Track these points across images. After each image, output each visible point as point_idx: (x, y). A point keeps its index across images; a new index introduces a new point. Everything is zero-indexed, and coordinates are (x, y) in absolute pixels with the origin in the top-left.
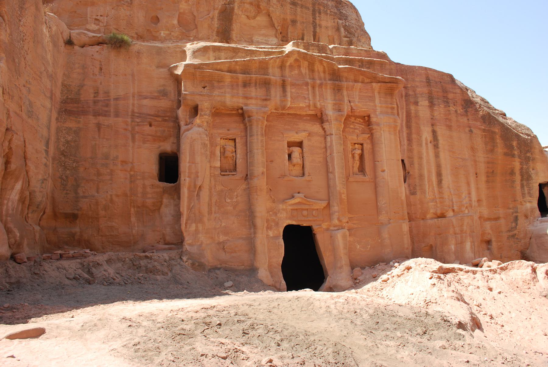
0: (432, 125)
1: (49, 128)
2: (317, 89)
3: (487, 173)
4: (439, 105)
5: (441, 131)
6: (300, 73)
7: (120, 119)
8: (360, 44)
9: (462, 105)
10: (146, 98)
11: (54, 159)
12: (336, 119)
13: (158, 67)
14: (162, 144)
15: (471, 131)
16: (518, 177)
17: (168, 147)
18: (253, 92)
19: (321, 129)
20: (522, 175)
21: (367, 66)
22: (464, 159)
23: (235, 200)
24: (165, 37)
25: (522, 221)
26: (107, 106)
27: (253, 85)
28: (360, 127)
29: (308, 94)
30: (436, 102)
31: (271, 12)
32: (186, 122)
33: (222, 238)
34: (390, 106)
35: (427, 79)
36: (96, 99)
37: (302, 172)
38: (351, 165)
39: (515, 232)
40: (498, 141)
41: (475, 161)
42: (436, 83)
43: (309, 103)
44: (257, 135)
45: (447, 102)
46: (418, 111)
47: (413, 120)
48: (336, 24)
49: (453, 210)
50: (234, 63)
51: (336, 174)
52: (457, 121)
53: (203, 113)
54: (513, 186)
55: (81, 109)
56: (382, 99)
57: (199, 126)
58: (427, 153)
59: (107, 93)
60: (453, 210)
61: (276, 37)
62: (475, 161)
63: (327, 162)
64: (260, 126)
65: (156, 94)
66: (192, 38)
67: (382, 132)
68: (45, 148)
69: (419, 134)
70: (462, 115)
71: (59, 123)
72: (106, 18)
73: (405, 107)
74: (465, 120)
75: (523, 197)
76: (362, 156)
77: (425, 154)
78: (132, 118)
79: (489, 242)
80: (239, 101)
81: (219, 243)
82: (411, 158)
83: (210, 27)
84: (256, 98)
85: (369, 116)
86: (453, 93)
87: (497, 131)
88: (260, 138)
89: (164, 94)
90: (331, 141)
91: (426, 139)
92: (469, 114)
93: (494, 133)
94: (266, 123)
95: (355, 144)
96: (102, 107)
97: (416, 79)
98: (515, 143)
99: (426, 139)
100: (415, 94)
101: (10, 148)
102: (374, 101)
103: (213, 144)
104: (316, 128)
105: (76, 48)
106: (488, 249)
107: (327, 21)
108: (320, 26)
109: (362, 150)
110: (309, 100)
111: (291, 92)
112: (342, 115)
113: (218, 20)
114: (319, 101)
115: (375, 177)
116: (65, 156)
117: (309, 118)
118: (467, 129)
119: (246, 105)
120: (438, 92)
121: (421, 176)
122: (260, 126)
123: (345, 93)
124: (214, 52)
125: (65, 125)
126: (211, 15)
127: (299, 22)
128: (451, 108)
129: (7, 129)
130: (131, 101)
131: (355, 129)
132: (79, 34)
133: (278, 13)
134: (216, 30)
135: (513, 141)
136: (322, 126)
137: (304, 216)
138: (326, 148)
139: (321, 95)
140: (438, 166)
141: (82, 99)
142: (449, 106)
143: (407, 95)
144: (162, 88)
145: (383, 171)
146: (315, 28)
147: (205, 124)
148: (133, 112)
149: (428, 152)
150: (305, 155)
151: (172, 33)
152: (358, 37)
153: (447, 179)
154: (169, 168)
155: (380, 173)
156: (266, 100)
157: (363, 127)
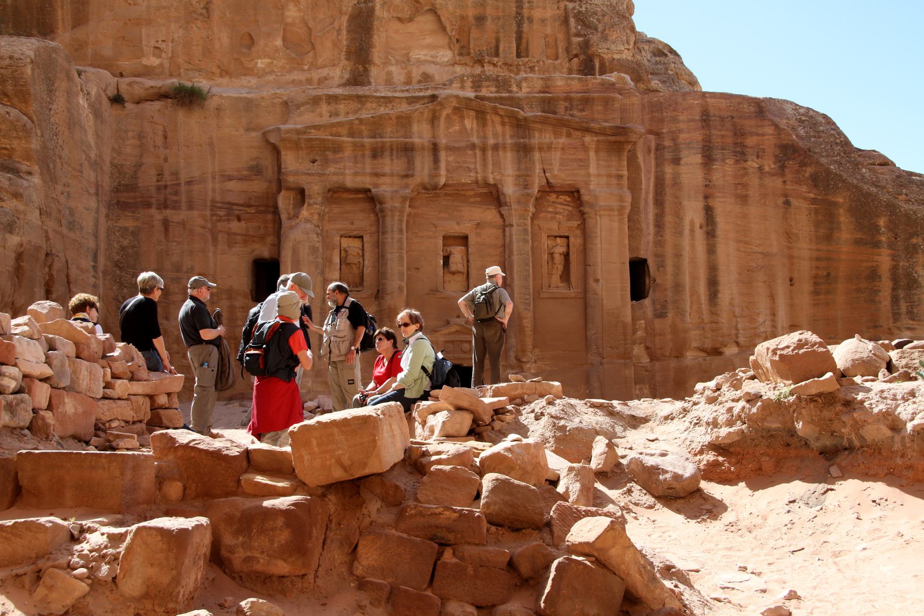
0: (706, 197)
1: (96, 236)
2: (489, 154)
3: (816, 277)
4: (723, 160)
5: (724, 207)
6: (463, 129)
7: (195, 213)
8: (604, 45)
9: (776, 156)
10: (230, 180)
11: (105, 273)
12: (519, 202)
13: (248, 130)
14: (256, 246)
15: (787, 203)
16: (885, 285)
17: (265, 252)
19: (498, 216)
20: (895, 279)
21: (580, 107)
22: (766, 255)
24: (263, 69)
26: (176, 193)
27: (387, 153)
28: (565, 210)
29: (475, 163)
30: (717, 154)
31: (438, 7)
32: (289, 214)
34: (614, 172)
35: (703, 115)
36: (160, 183)
37: (465, 284)
38: (545, 270)
40: (842, 219)
41: (791, 257)
42: (722, 119)
43: (477, 177)
44: (392, 231)
45: (741, 154)
46: (679, 174)
47: (669, 191)
48: (562, 11)
49: (737, 344)
50: (357, 122)
52: (762, 186)
53: (312, 201)
54: (873, 301)
55: (139, 200)
56: (602, 163)
57: (307, 221)
58: (693, 247)
59: (175, 174)
60: (737, 344)
61: (450, 49)
62: (791, 257)
64: (396, 218)
65: (246, 173)
66: (306, 67)
67: (598, 218)
68: (92, 264)
69: (678, 215)
70: (773, 175)
71: (110, 222)
72: (171, 44)
73: (653, 170)
74: (778, 182)
75: (896, 320)
76: (567, 256)
78: (212, 210)
80: (366, 181)
82: (660, 256)
83: (335, 45)
84: (392, 175)
85: (578, 191)
86: (758, 135)
87: (841, 200)
88: (396, 236)
89: (256, 171)
90: (511, 236)
91: (692, 223)
92: (787, 171)
93: (836, 204)
94: (408, 210)
95: (556, 237)
96: (168, 195)
97: (681, 118)
98: (882, 222)
99: (692, 223)
100: (676, 145)
101: (51, 276)
102: (587, 167)
103: (328, 246)
104: (490, 215)
105: (129, 106)
107: (545, 8)
108: (530, 20)
109: (568, 246)
110: (477, 173)
111: (447, 161)
112: (528, 195)
113: (348, 32)
114: (492, 173)
115: (585, 290)
116: (120, 268)
117: (479, 199)
118: (780, 201)
119: (377, 186)
120: (723, 136)
121: (678, 287)
122: (396, 218)
123: (537, 156)
124: (329, 104)
125: (118, 224)
126: (336, 25)
127: (489, 19)
128: (749, 163)
129: (47, 255)
130: (210, 185)
131: (556, 213)
132: (130, 84)
133: (450, 8)
134: (345, 49)
135: (878, 216)
136: (500, 212)
137: (464, 352)
139: (497, 164)
141: (140, 185)
142: (745, 161)
143: (659, 148)
144: (254, 163)
145: (597, 281)
146: (519, 24)
147: (316, 217)
148: (213, 201)
149: (693, 246)
150: (471, 258)
151: (275, 62)
152: (602, 33)
153: (729, 290)
155: (592, 283)
156: (406, 176)
157: (570, 209)
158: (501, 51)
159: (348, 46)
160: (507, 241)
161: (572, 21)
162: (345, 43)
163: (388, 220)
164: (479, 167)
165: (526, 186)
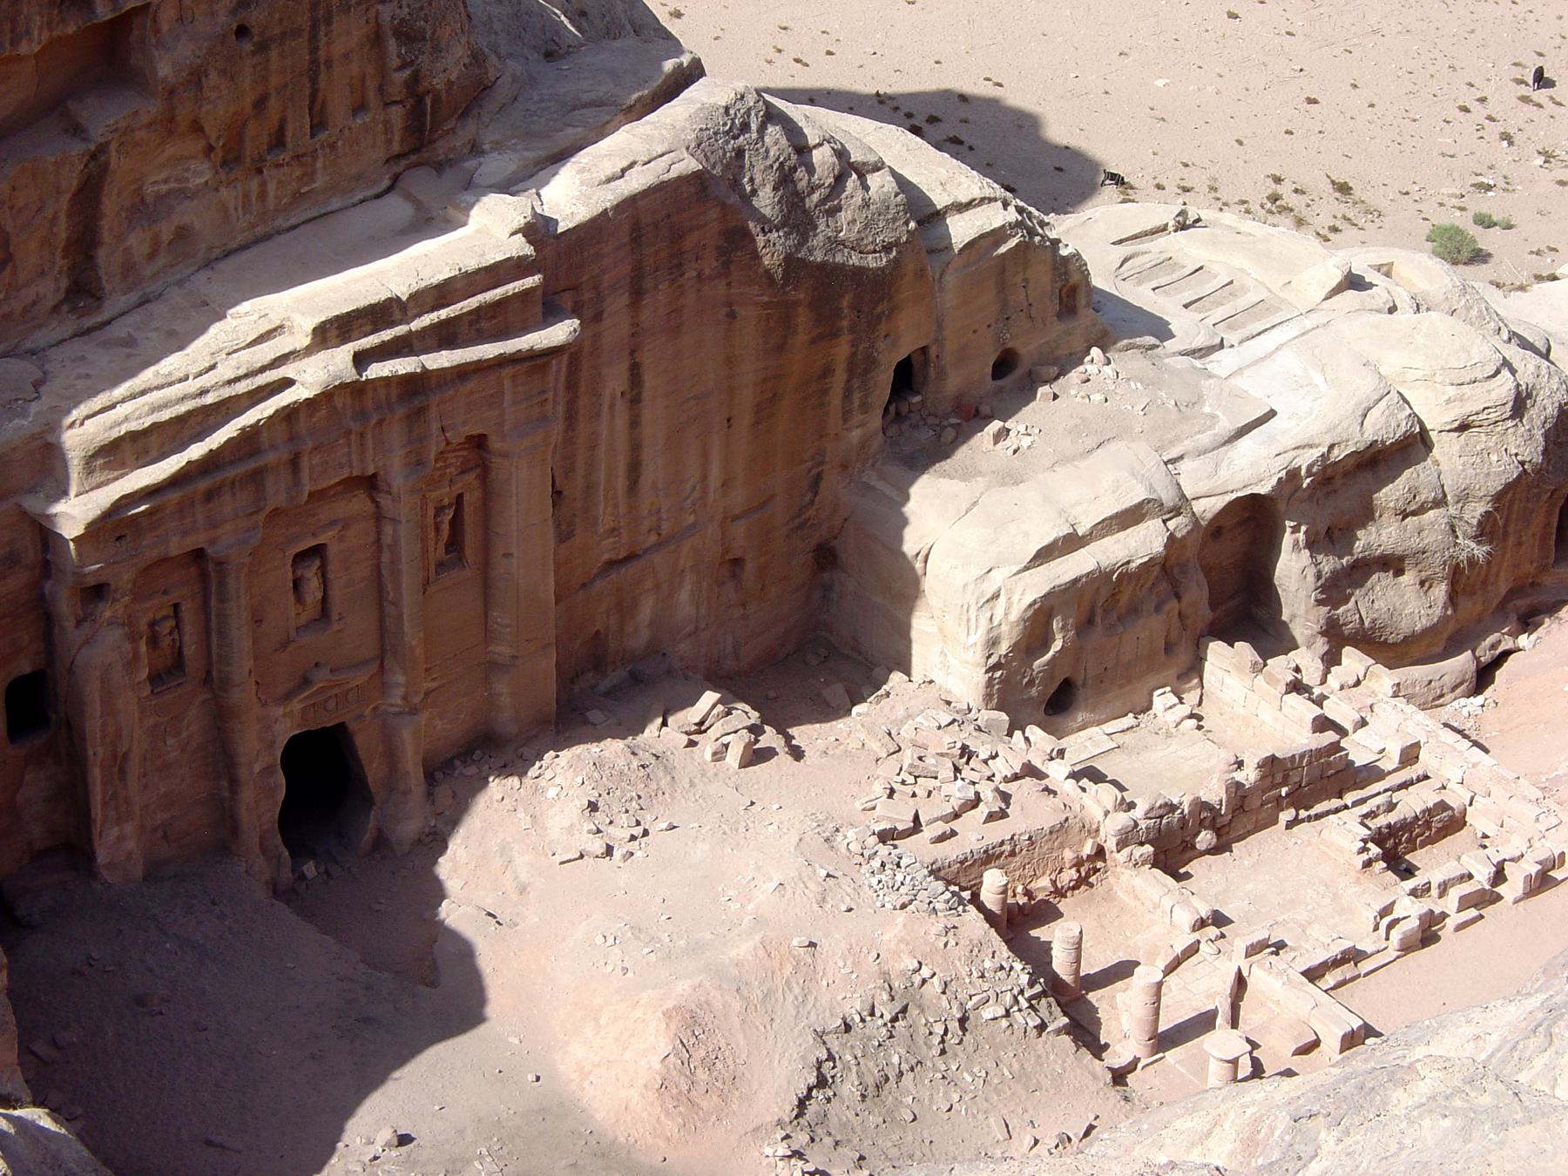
0: (632, 352)
4: (656, 287)
16: (840, 376)
18: (227, 505)
20: (851, 370)
23: (184, 735)
25: (833, 483)
29: (349, 454)
30: (648, 283)
33: (160, 818)
39: (811, 512)
51: (406, 611)
63: (379, 575)
77: (605, 434)
79: (737, 562)
81: (155, 830)
86: (699, 228)
106: (734, 576)
121: (590, 488)
123: (433, 413)
126: (49, 212)
131: (446, 467)
138: (378, 541)
140: (635, 448)
153: (654, 470)
158: (289, 134)
159: (68, 238)
160: (387, 539)
161: (392, 45)
162: (64, 235)
163: (231, 582)
164: (355, 457)
165: (420, 463)
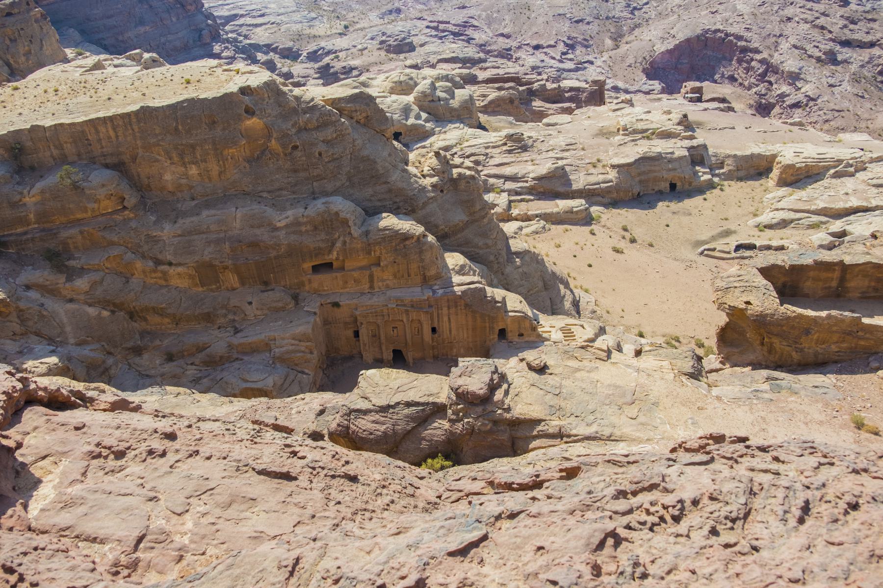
45: (456, 307)
154: (357, 334)
